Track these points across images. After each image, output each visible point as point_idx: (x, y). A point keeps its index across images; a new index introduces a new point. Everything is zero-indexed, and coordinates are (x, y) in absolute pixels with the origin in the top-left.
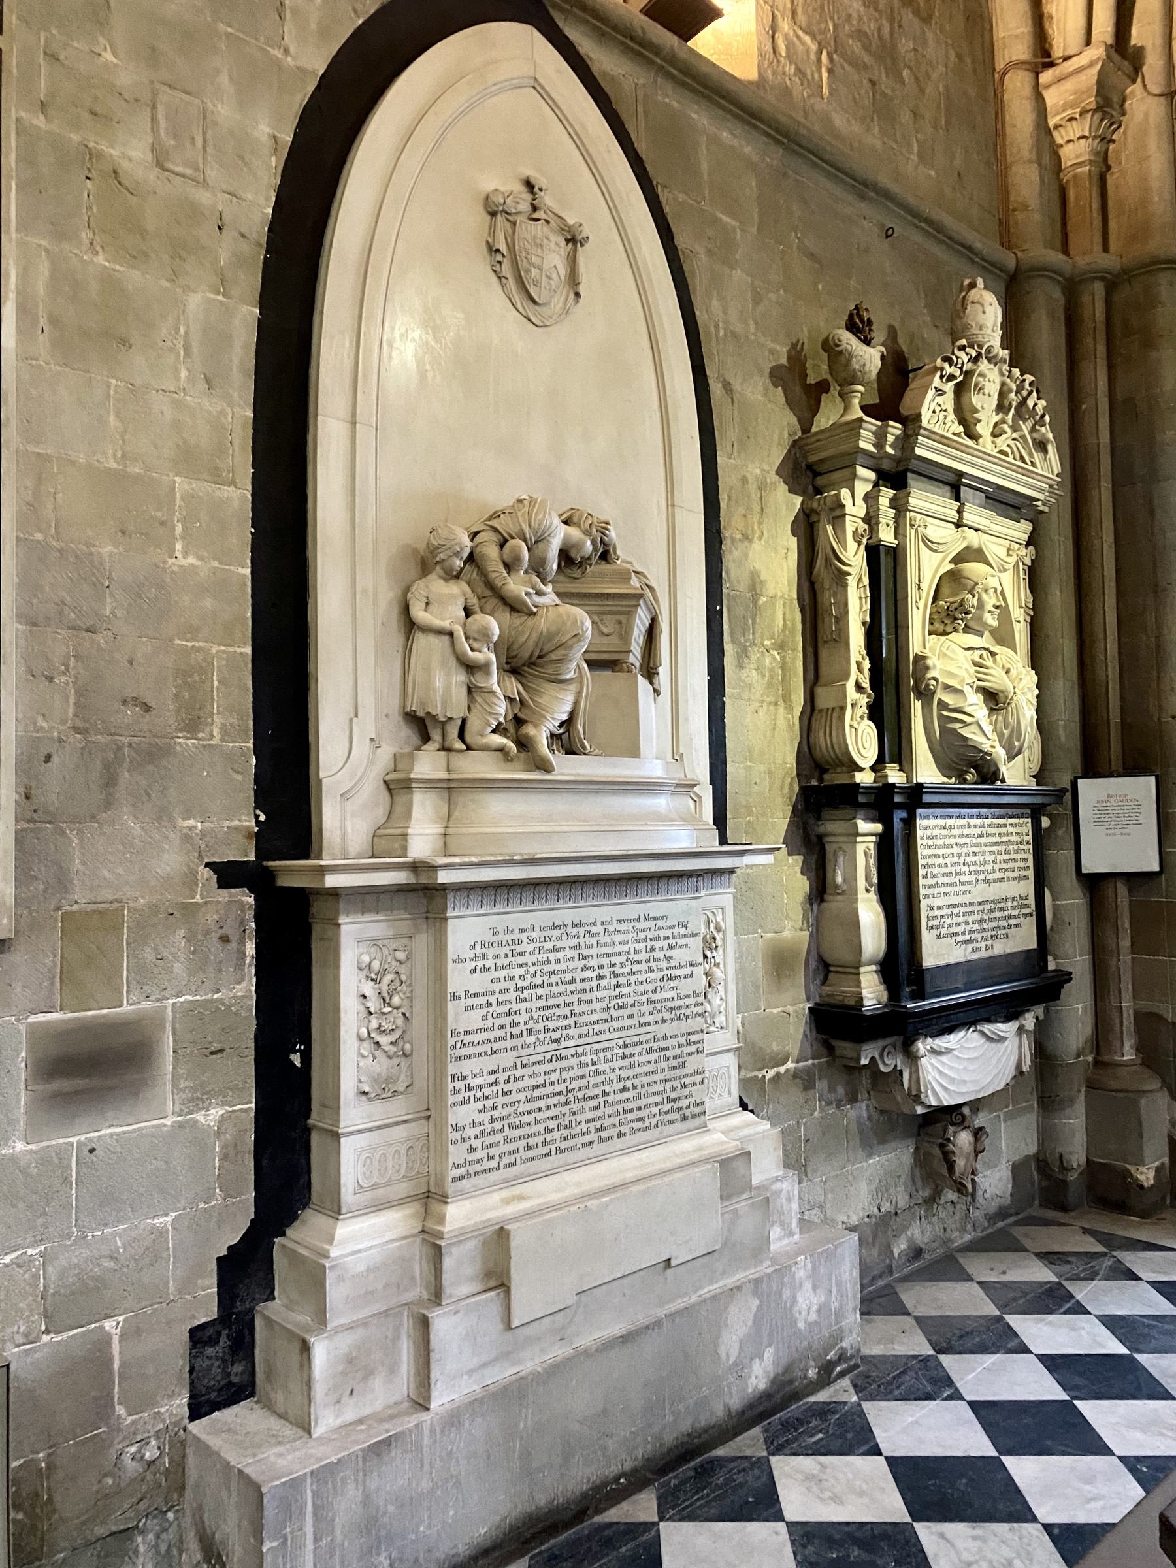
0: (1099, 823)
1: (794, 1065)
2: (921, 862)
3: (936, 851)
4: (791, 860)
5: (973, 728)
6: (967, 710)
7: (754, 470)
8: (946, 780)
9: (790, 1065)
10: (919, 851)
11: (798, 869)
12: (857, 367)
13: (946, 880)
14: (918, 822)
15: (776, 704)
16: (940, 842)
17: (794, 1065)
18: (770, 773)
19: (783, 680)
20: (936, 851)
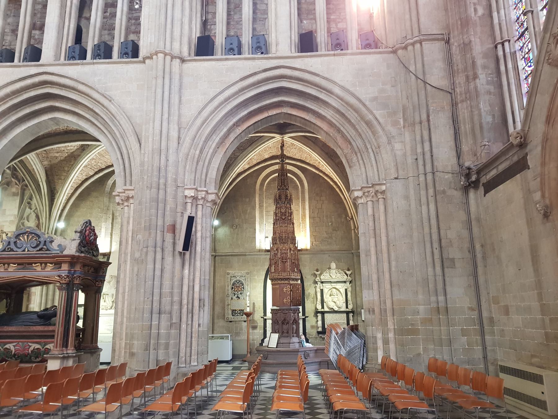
7: (309, 284)
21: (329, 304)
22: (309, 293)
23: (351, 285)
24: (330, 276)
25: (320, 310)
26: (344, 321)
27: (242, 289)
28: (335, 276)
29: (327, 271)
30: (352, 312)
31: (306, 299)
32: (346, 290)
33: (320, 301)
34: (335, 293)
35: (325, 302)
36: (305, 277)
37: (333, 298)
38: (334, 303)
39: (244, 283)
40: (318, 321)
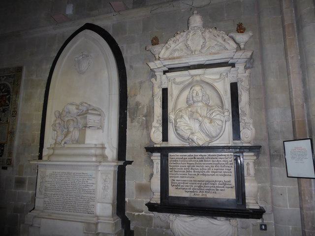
0: (293, 158)
2: (169, 167)
9: (143, 213)
16: (179, 162)
18: (140, 145)
22: (138, 104)
25: (158, 146)
26: (227, 179)
27: (7, 102)
30: (255, 149)
31: (128, 119)
32: (234, 87)
36: (131, 67)
39: (11, 90)
40: (152, 175)
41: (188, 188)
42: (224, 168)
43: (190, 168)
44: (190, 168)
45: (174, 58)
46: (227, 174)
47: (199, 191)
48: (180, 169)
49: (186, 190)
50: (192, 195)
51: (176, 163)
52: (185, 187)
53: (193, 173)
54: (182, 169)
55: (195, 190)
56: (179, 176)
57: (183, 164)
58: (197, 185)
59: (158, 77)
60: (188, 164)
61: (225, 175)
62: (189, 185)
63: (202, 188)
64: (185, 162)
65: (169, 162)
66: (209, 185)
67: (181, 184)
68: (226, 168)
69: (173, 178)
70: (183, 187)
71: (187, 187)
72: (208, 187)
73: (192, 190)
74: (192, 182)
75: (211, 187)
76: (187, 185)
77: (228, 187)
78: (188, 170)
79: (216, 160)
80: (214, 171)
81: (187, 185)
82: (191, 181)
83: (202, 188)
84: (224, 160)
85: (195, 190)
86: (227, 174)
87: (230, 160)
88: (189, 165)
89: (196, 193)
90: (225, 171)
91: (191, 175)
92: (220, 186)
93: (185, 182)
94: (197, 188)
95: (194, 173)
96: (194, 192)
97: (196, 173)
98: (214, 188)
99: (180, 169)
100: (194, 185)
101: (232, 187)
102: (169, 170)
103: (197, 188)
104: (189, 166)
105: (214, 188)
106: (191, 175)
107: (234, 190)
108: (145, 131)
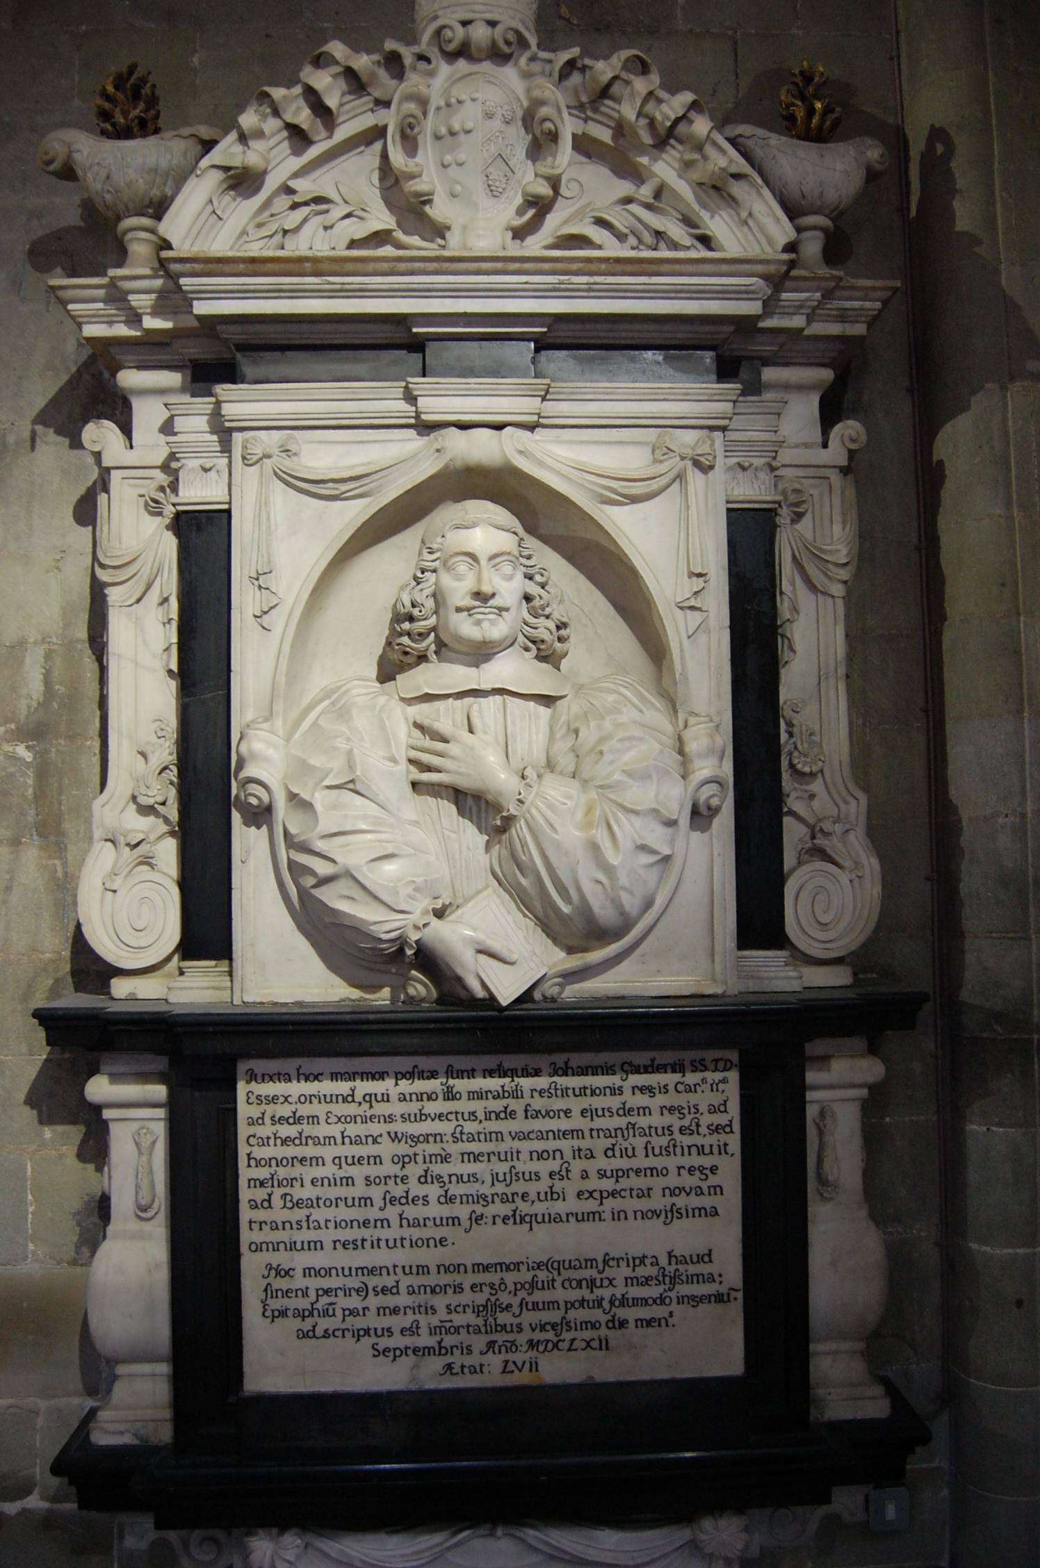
1: (45, 1505)
2: (245, 1173)
3: (310, 1151)
4: (48, 1132)
5: (342, 886)
6: (320, 845)
8: (355, 994)
9: (34, 1502)
10: (243, 1150)
11: (70, 1150)
12: (99, 186)
13: (344, 1213)
14: (242, 1088)
15: (15, 842)
16: (322, 1130)
17: (45, 1505)
19: (39, 796)
20: (310, 1151)
21: (350, 855)
23: (848, 430)
24: (382, 219)
28: (507, 211)
29: (322, 80)
33: (165, 792)
34: (508, 587)
35: (261, 815)
37: (444, 716)
38: (470, 837)
41: (396, 1322)
42: (671, 1162)
43: (414, 1170)
44: (414, 1170)
45: (296, 266)
46: (695, 1201)
47: (479, 1342)
48: (333, 1182)
49: (384, 1342)
50: (430, 1375)
51: (302, 1140)
52: (372, 1321)
53: (435, 1210)
54: (349, 1181)
55: (449, 1340)
56: (328, 1236)
57: (358, 1141)
58: (467, 1297)
59: (147, 415)
60: (395, 1137)
61: (673, 1213)
62: (403, 1300)
63: (504, 1318)
64: (375, 1128)
65: (243, 1130)
66: (560, 1294)
67: (343, 1302)
68: (687, 1161)
69: (281, 1258)
70: (360, 1323)
71: (387, 1321)
72: (551, 1305)
73: (431, 1341)
74: (431, 1280)
75: (570, 1305)
76: (391, 1301)
77: (695, 1300)
78: (398, 1191)
79: (614, 1102)
80: (594, 1183)
81: (391, 1301)
82: (423, 1269)
83: (504, 1318)
84: (672, 1099)
85: (449, 1340)
86: (695, 1201)
87: (716, 1099)
88: (403, 1149)
89: (457, 1359)
90: (673, 1180)
91: (415, 1223)
92: (636, 1292)
93: (373, 1282)
94: (469, 1318)
95: (446, 1211)
96: (441, 1350)
97: (463, 1211)
98: (598, 1315)
99: (333, 1182)
100: (440, 1302)
101: (720, 1298)
102: (245, 1194)
103: (469, 1318)
104: (402, 1161)
105: (598, 1315)
106: (415, 1223)
107: (735, 1310)
108: (31, 855)
